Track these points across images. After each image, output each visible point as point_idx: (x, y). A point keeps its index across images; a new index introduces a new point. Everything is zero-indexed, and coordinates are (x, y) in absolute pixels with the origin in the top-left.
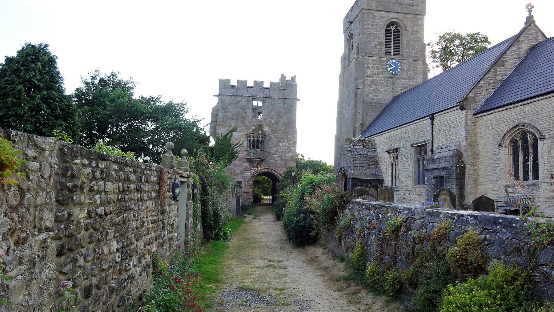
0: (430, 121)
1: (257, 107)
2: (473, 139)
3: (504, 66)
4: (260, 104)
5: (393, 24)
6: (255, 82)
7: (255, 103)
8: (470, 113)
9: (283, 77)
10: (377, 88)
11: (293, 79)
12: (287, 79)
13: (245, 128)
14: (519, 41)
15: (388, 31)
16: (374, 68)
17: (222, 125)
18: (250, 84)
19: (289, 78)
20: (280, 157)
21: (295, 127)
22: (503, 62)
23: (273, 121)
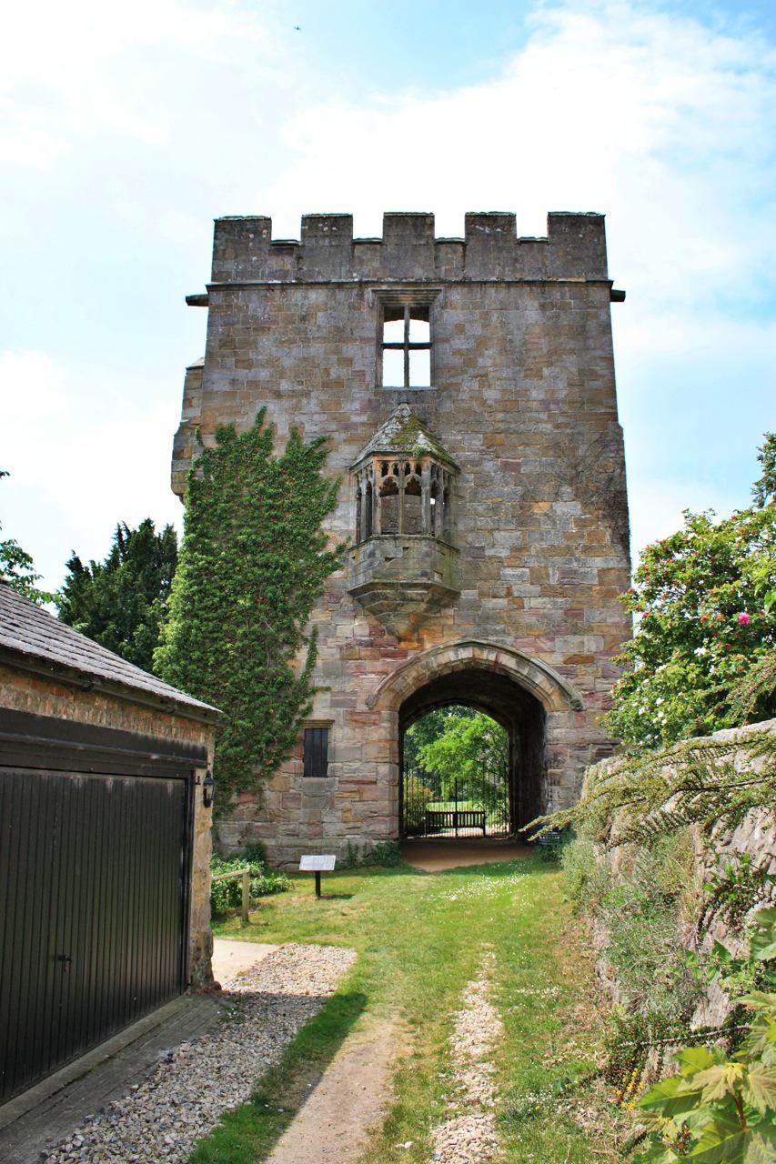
20: (537, 578)
23: (491, 395)
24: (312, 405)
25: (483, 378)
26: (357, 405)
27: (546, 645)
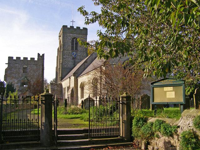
5: (75, 38)
11: (43, 55)
15: (73, 41)
18: (22, 59)
24: (17, 74)
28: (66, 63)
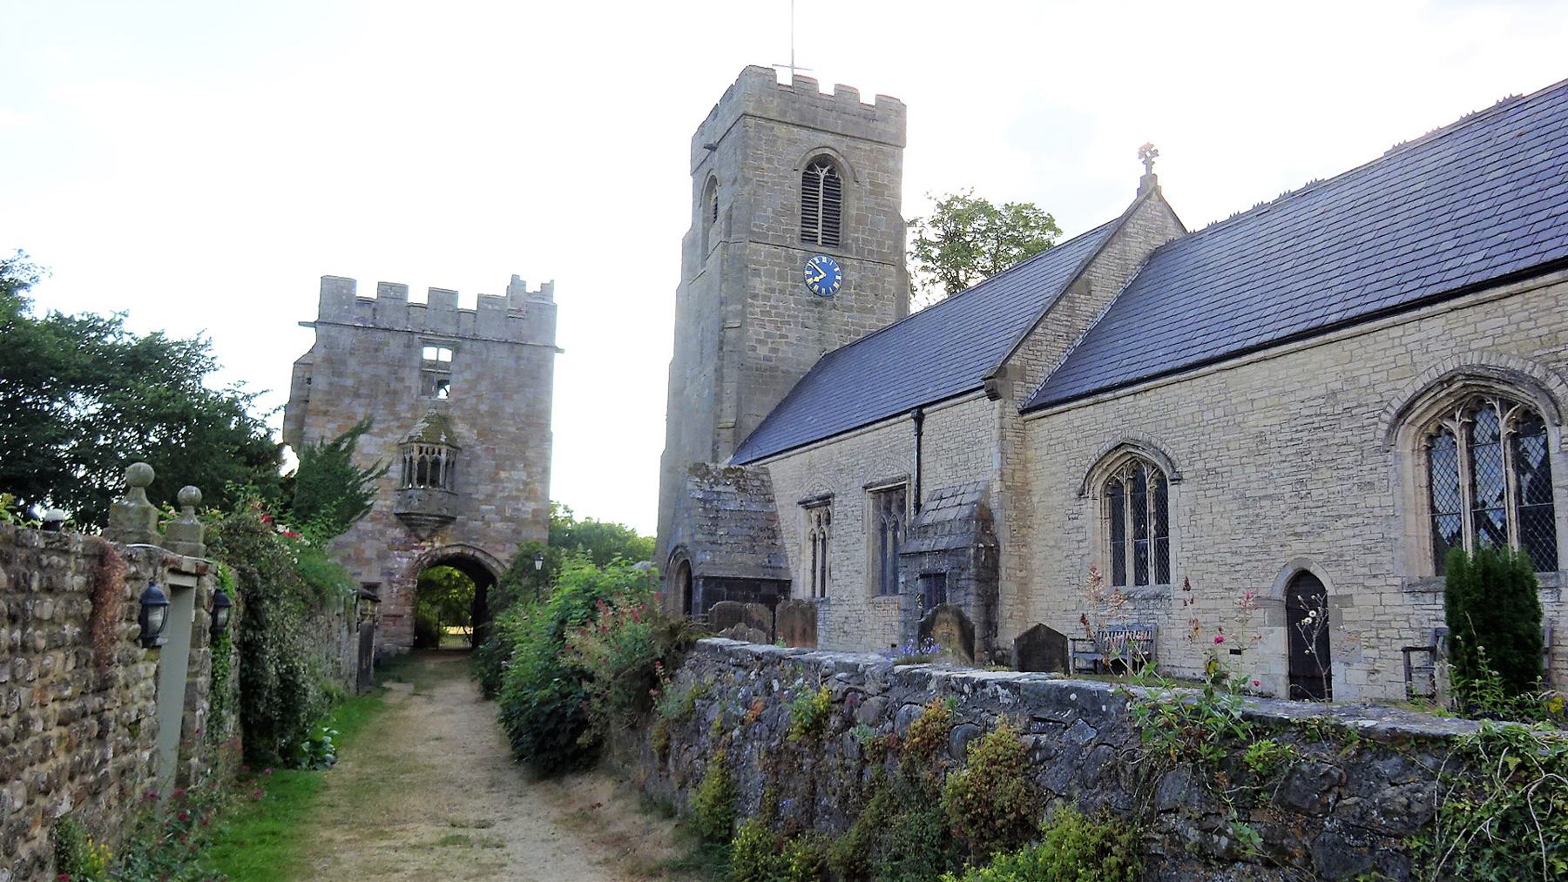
0: (912, 424)
1: (436, 364)
2: (1018, 474)
3: (1090, 293)
4: (446, 355)
5: (822, 161)
6: (433, 292)
7: (429, 353)
8: (1012, 409)
9: (516, 283)
10: (778, 328)
11: (547, 289)
12: (529, 289)
13: (395, 424)
14: (1125, 234)
15: (809, 180)
16: (771, 275)
17: (326, 413)
19: (532, 287)
21: (548, 425)
22: (1089, 283)
23: (483, 408)
25: (479, 397)
26: (404, 407)
27: (500, 547)
28: (770, 328)
